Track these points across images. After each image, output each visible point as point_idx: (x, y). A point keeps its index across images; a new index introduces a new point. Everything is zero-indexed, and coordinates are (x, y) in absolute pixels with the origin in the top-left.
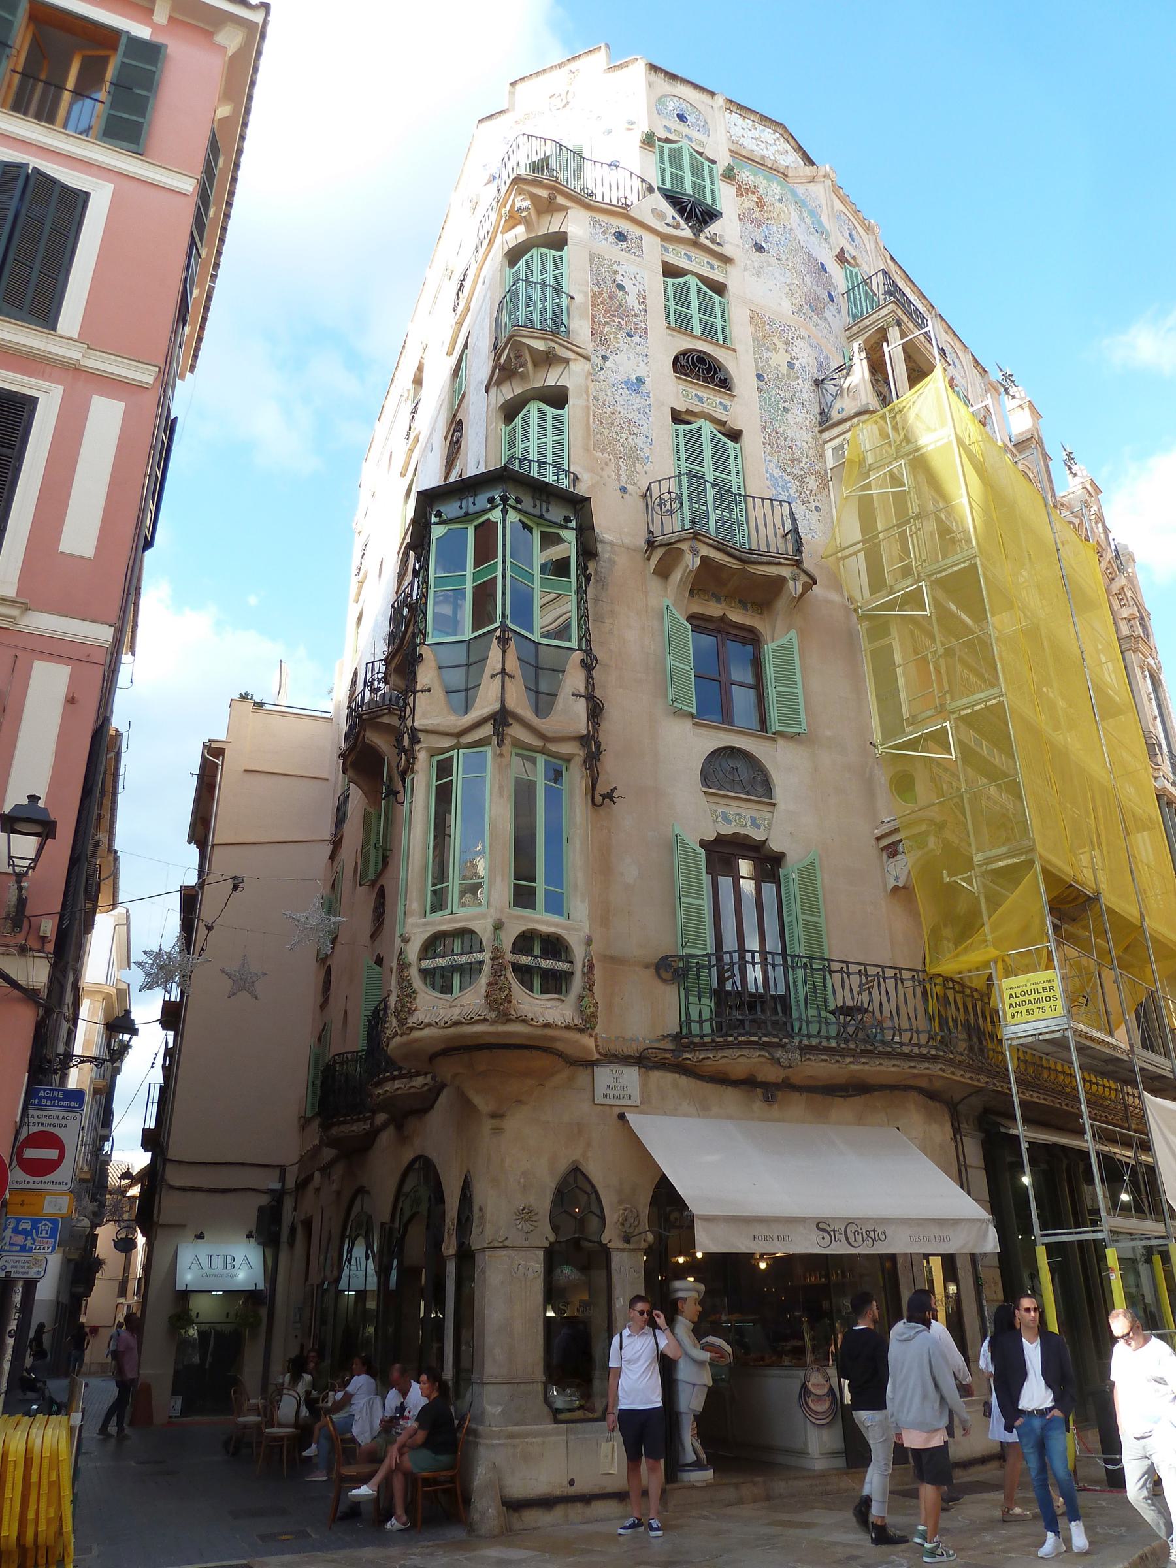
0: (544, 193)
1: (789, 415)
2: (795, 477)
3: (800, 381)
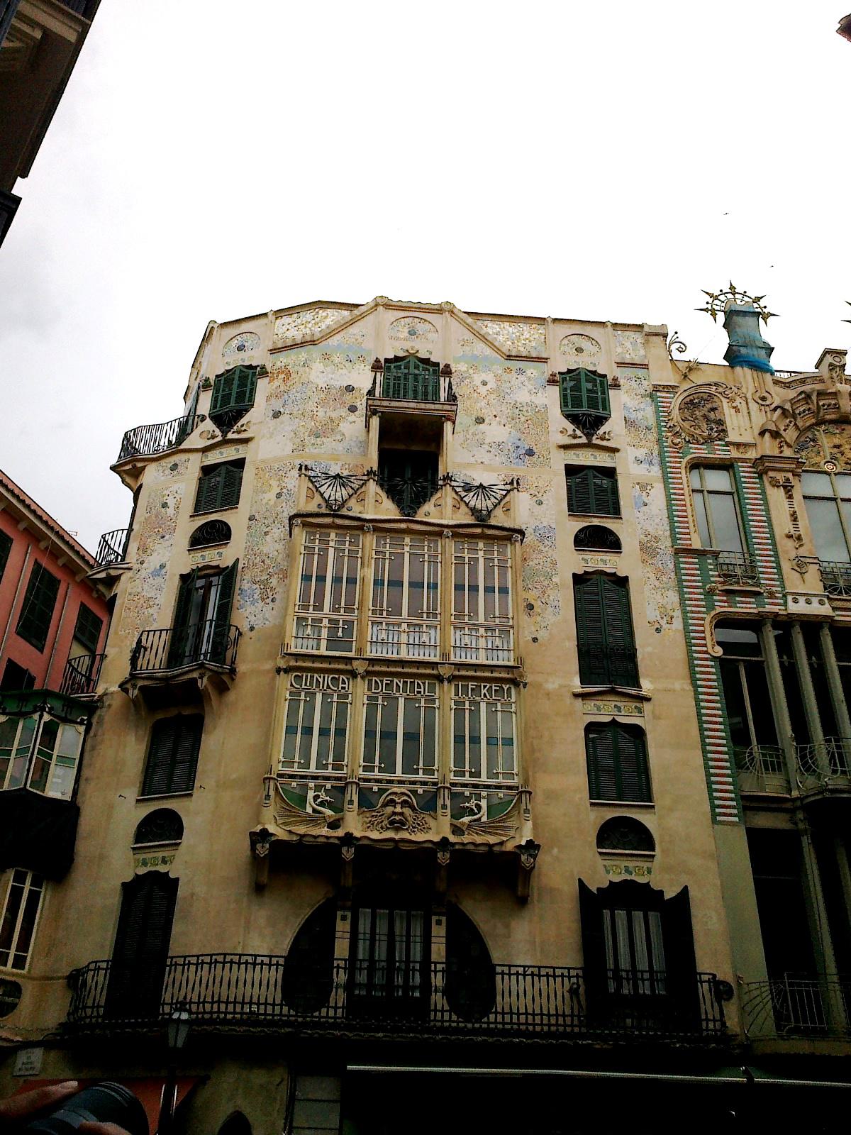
0: (129, 467)
3: (284, 504)
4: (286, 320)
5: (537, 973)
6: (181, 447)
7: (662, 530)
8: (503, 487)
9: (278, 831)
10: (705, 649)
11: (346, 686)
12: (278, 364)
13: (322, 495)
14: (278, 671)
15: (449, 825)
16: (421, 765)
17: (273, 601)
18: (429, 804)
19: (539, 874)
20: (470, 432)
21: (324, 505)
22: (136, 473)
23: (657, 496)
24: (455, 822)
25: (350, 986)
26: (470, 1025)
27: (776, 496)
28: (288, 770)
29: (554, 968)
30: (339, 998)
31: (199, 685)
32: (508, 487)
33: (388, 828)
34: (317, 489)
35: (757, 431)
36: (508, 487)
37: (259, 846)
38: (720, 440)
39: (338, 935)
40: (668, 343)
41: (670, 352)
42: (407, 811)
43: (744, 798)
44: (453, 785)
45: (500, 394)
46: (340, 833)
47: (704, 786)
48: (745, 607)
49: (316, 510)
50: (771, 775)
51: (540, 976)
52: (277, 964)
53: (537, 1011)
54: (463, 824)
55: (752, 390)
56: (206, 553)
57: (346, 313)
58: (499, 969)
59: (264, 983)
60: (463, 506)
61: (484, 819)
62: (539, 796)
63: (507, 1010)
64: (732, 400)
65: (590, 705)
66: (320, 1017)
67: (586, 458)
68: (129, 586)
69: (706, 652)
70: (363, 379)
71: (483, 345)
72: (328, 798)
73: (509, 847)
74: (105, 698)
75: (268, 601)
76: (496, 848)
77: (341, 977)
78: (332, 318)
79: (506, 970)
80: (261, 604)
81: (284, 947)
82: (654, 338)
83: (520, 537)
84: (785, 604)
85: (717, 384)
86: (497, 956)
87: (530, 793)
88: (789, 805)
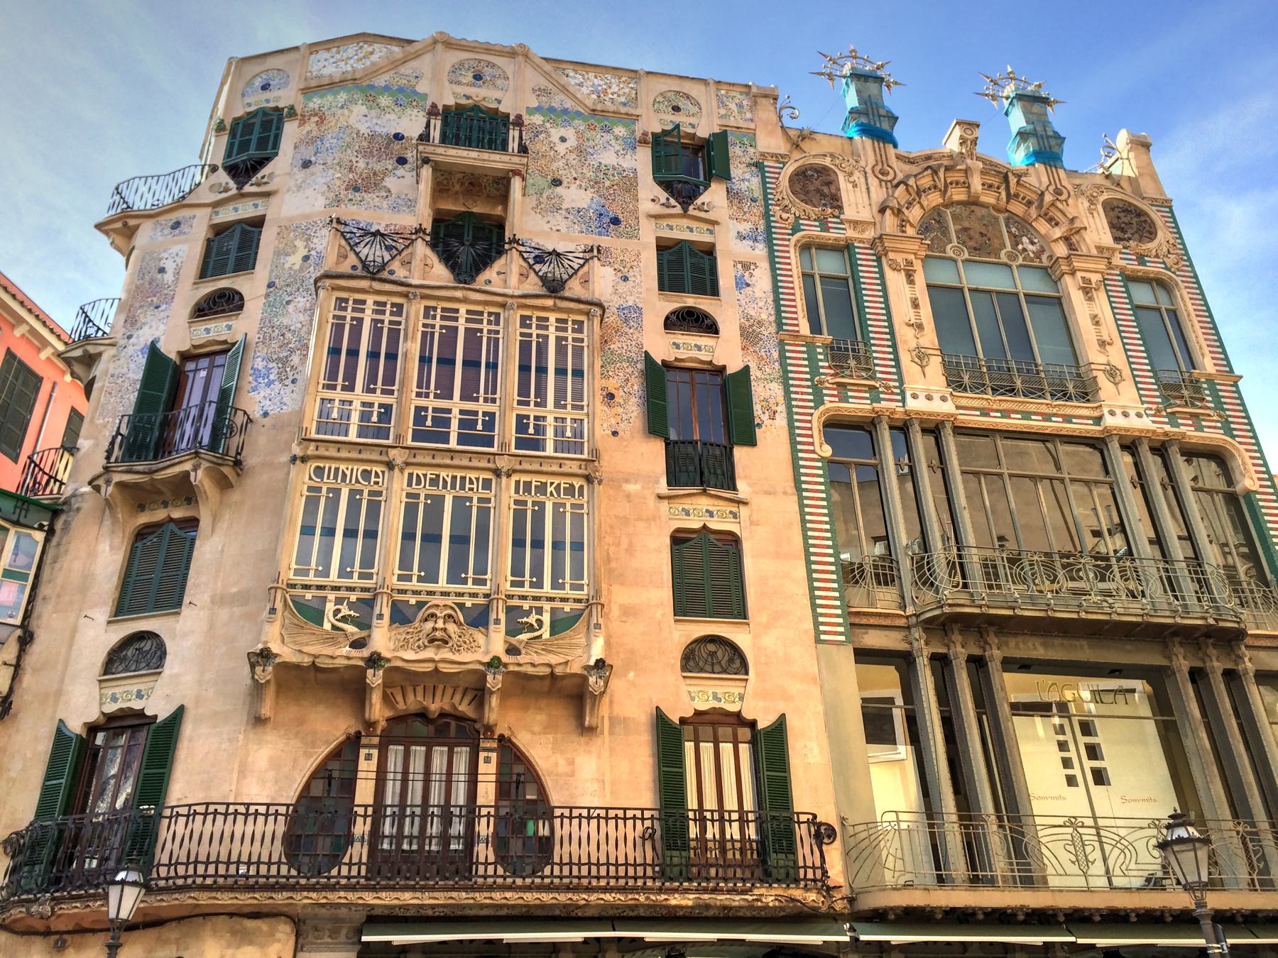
1: (291, 308)
2: (279, 359)
4: (323, 55)
5: (606, 815)
6: (185, 202)
7: (767, 315)
8: (581, 255)
9: (285, 652)
10: (811, 448)
11: (380, 480)
12: (311, 105)
13: (357, 254)
14: (294, 459)
15: (502, 642)
16: (470, 573)
17: (294, 381)
18: (479, 618)
19: (611, 702)
20: (545, 196)
21: (360, 266)
22: (129, 232)
23: (761, 280)
24: (513, 640)
25: (376, 835)
26: (519, 881)
27: (895, 280)
28: (301, 580)
29: (625, 810)
30: (359, 852)
31: (192, 479)
32: (587, 256)
33: (425, 647)
34: (352, 249)
35: (875, 209)
36: (587, 256)
37: (259, 669)
38: (834, 217)
39: (360, 775)
40: (778, 106)
41: (780, 117)
42: (452, 628)
43: (850, 613)
44: (510, 597)
45: (580, 151)
46: (365, 653)
47: (807, 602)
48: (858, 405)
49: (350, 271)
50: (884, 589)
51: (607, 818)
52: (277, 814)
53: (603, 860)
54: (521, 642)
55: (871, 161)
56: (211, 325)
57: (396, 49)
58: (558, 812)
59: (258, 837)
60: (532, 275)
61: (546, 635)
62: (615, 612)
63: (566, 860)
64: (851, 174)
65: (679, 506)
66: (328, 878)
67: (682, 231)
68: (112, 366)
69: (813, 452)
70: (412, 124)
71: (562, 97)
72: (352, 613)
73: (575, 668)
74: (73, 500)
75: (288, 382)
76: (559, 671)
77: (361, 828)
78: (379, 53)
79: (567, 812)
80: (277, 386)
81: (290, 795)
82: (764, 101)
83: (599, 312)
84: (903, 400)
85: (832, 155)
86: (556, 798)
87: (603, 605)
88: (902, 622)
